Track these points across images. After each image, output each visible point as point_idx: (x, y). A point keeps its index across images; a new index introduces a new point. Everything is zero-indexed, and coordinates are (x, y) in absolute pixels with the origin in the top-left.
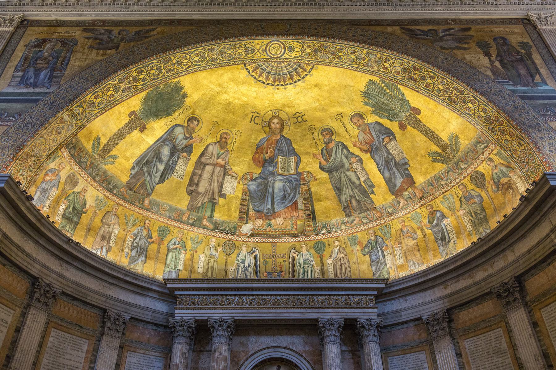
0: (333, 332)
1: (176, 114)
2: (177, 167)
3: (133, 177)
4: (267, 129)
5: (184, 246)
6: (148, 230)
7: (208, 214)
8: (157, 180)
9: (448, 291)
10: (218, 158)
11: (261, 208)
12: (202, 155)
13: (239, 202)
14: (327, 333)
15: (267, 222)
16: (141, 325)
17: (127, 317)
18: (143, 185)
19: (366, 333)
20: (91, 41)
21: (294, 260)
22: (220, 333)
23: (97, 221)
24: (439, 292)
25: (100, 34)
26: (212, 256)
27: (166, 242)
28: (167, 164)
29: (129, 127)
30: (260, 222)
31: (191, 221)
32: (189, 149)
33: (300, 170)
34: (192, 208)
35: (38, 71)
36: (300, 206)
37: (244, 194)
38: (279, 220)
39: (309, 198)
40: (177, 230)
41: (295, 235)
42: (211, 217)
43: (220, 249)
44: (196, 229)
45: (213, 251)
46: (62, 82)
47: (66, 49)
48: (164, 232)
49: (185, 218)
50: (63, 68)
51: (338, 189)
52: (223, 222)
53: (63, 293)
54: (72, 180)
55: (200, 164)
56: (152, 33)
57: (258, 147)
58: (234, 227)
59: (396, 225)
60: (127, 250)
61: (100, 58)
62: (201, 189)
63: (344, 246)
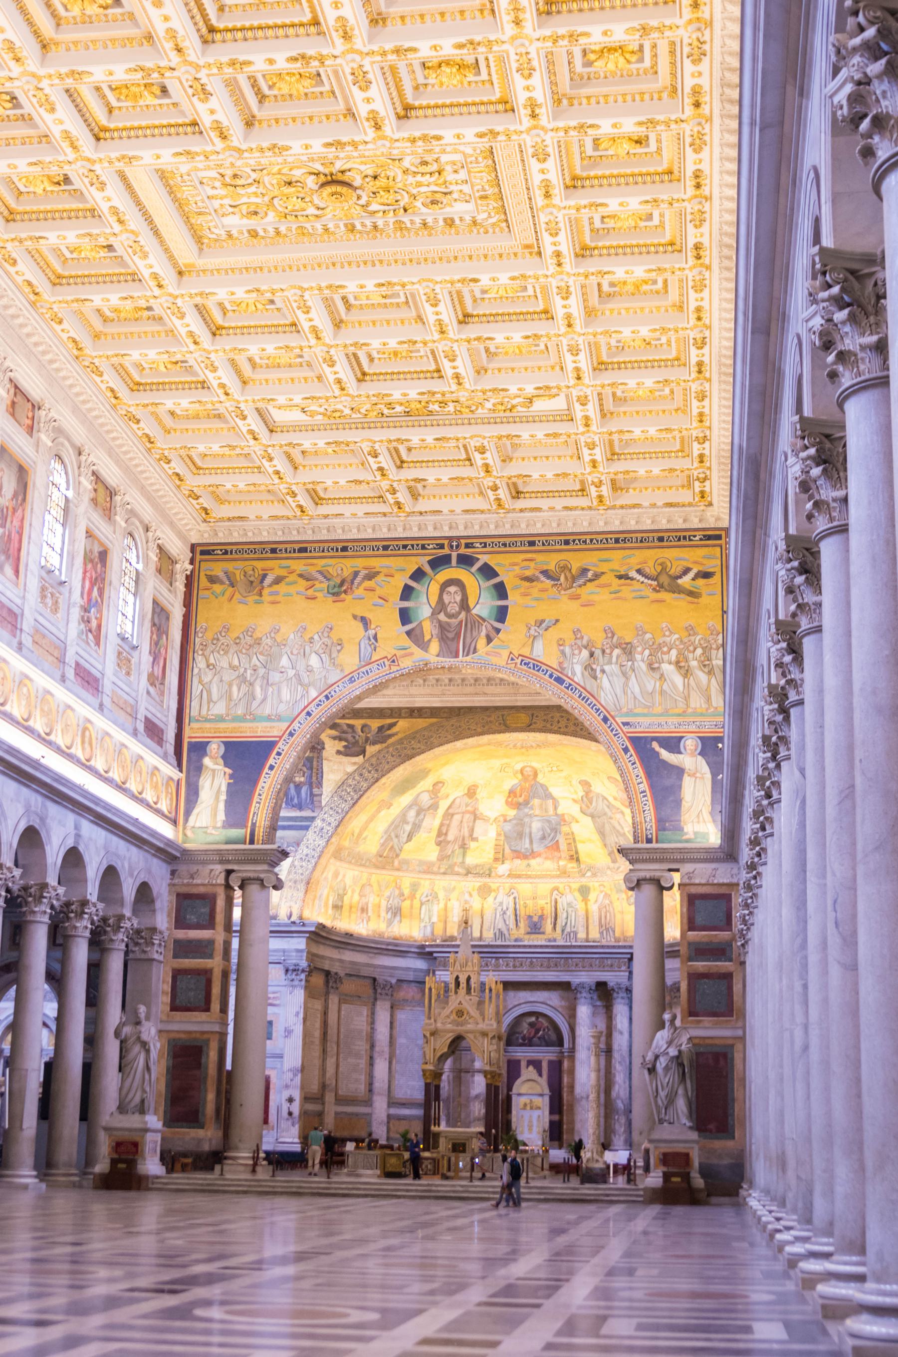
0: (584, 995)
1: (422, 783)
2: (424, 824)
3: (383, 845)
4: (520, 776)
6: (399, 888)
7: (460, 860)
8: (405, 840)
10: (467, 805)
11: (518, 848)
12: (450, 807)
13: (493, 843)
14: (579, 995)
15: (525, 862)
16: (405, 985)
17: (394, 981)
18: (392, 847)
19: (615, 995)
20: (337, 742)
21: (556, 902)
23: (356, 897)
25: (344, 732)
26: (466, 902)
27: (418, 896)
28: (414, 824)
29: (378, 811)
30: (518, 862)
31: (442, 870)
32: (434, 807)
33: (560, 811)
34: (441, 858)
35: (298, 787)
36: (563, 846)
37: (499, 834)
38: (538, 860)
39: (572, 840)
40: (428, 882)
41: (558, 877)
42: (463, 862)
43: (475, 893)
44: (447, 877)
45: (467, 897)
46: (323, 803)
47: (315, 755)
48: (415, 887)
49: (435, 869)
50: (320, 785)
51: (602, 833)
52: (477, 866)
53: (348, 975)
54: (336, 874)
55: (448, 815)
56: (394, 730)
57: (512, 792)
58: (490, 870)
60: (383, 914)
61: (350, 769)
62: (450, 837)
63: (609, 892)
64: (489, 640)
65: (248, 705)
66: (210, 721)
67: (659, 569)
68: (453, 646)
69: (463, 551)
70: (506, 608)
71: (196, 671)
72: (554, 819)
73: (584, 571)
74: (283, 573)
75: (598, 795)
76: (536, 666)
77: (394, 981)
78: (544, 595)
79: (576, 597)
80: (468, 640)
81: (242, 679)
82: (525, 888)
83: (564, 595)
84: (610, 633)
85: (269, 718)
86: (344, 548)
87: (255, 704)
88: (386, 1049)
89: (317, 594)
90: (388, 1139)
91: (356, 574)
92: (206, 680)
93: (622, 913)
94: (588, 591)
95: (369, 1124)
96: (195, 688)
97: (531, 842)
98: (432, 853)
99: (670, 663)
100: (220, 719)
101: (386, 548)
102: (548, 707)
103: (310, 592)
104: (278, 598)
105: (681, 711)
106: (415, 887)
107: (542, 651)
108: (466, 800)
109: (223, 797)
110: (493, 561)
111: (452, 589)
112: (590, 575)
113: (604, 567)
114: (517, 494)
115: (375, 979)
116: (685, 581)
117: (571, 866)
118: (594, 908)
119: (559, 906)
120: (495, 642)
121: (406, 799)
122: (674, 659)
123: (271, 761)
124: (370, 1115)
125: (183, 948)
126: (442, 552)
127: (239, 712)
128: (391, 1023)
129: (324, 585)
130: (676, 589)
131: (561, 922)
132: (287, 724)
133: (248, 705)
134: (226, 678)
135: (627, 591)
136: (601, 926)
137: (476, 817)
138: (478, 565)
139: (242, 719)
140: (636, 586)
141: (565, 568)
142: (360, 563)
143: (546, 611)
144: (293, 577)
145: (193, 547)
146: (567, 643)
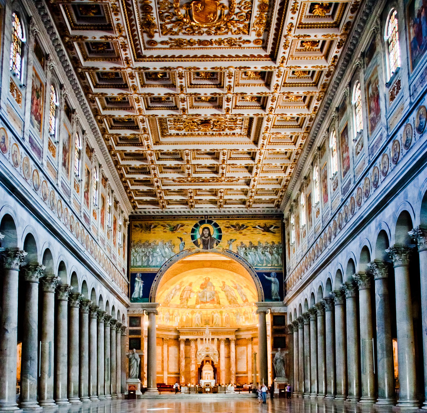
5: (179, 314)
9: (253, 333)
16: (171, 340)
17: (168, 339)
22: (193, 342)
24: (251, 332)
29: (165, 290)
30: (202, 304)
32: (180, 289)
33: (215, 290)
34: (181, 303)
36: (215, 300)
37: (197, 296)
38: (208, 304)
39: (218, 298)
45: (187, 314)
51: (227, 296)
55: (184, 291)
57: (202, 285)
59: (243, 310)
62: (184, 297)
64: (217, 245)
65: (148, 262)
66: (136, 267)
67: (264, 225)
68: (207, 246)
69: (209, 219)
70: (221, 235)
71: (132, 253)
72: (213, 292)
73: (243, 225)
74: (156, 224)
75: (227, 285)
76: (230, 252)
77: (168, 339)
78: (232, 232)
79: (241, 233)
80: (211, 244)
81: (146, 255)
82: (204, 312)
83: (238, 232)
84: (251, 243)
85: (154, 266)
86: (174, 217)
87: (150, 263)
88: (167, 358)
89: (167, 231)
90: (168, 383)
91: (178, 225)
92: (135, 255)
93: (232, 319)
94: (244, 231)
95: (163, 379)
96: (132, 258)
97: (206, 299)
98: (178, 302)
99: (267, 252)
100: (140, 267)
101: (186, 218)
102: (216, 261)
103: (165, 230)
104: (156, 232)
105: (271, 265)
106: (173, 312)
107: (233, 248)
108: (189, 287)
109: (142, 289)
110: (218, 222)
111: (206, 230)
112: (245, 226)
113: (249, 225)
114: (226, 203)
115: (163, 339)
116: (271, 229)
117: (218, 305)
118: (224, 317)
119: (214, 317)
120: (219, 245)
121: (173, 287)
122: (269, 251)
123: (155, 279)
124: (163, 377)
125: (131, 332)
126: (203, 219)
127: (145, 264)
128: (168, 351)
129: (169, 228)
130: (268, 231)
131: (214, 321)
132: (159, 268)
133: (148, 262)
134: (141, 255)
135: (255, 232)
136: (226, 322)
137: (191, 291)
138: (213, 223)
139: (146, 267)
140: (258, 230)
141: (238, 225)
142: (178, 222)
143: (233, 237)
144: (159, 226)
145: (130, 217)
146: (239, 246)
